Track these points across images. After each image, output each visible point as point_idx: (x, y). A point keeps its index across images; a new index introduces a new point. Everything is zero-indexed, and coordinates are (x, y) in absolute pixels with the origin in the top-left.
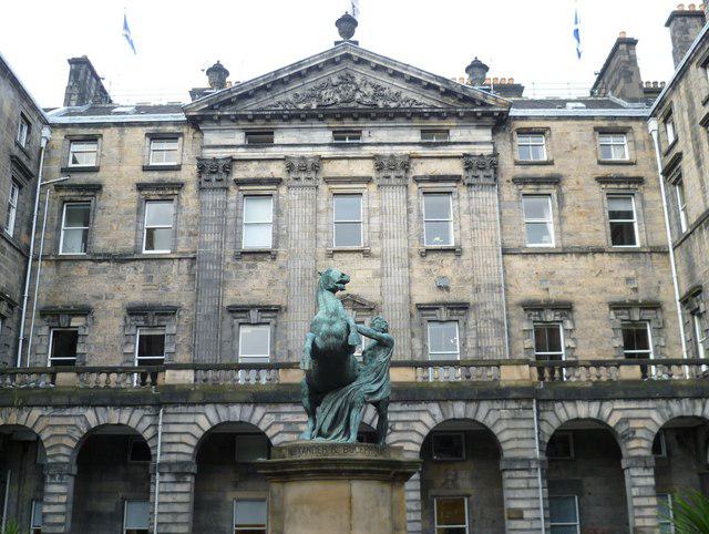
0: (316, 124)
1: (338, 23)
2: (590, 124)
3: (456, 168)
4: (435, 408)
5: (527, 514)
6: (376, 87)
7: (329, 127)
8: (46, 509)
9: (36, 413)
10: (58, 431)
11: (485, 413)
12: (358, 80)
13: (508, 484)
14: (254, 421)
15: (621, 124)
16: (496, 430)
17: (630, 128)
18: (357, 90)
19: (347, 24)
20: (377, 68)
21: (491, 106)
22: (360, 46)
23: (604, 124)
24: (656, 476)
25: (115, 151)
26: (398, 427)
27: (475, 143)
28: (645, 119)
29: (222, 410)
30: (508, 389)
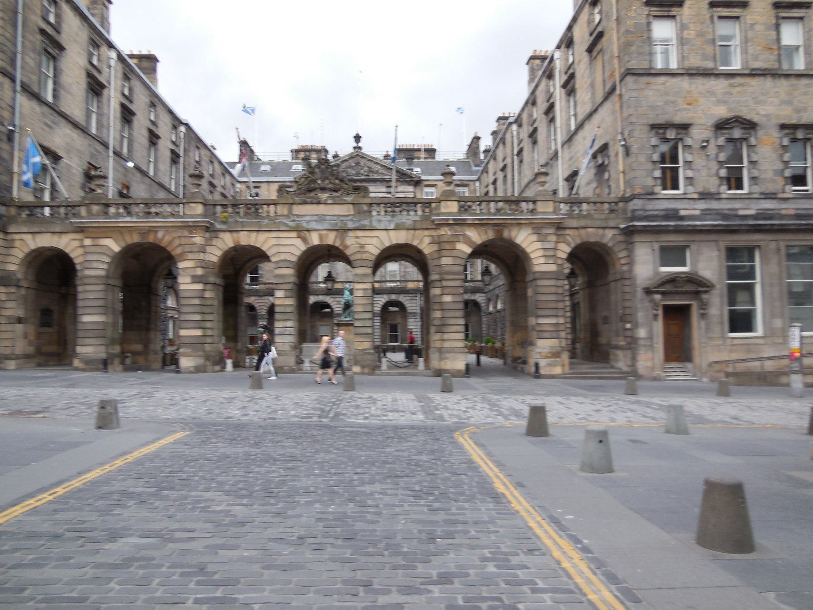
4: (385, 296)
6: (369, 168)
9: (253, 298)
10: (262, 304)
11: (402, 298)
12: (362, 164)
15: (465, 183)
19: (358, 138)
20: (370, 160)
23: (458, 183)
30: (409, 290)
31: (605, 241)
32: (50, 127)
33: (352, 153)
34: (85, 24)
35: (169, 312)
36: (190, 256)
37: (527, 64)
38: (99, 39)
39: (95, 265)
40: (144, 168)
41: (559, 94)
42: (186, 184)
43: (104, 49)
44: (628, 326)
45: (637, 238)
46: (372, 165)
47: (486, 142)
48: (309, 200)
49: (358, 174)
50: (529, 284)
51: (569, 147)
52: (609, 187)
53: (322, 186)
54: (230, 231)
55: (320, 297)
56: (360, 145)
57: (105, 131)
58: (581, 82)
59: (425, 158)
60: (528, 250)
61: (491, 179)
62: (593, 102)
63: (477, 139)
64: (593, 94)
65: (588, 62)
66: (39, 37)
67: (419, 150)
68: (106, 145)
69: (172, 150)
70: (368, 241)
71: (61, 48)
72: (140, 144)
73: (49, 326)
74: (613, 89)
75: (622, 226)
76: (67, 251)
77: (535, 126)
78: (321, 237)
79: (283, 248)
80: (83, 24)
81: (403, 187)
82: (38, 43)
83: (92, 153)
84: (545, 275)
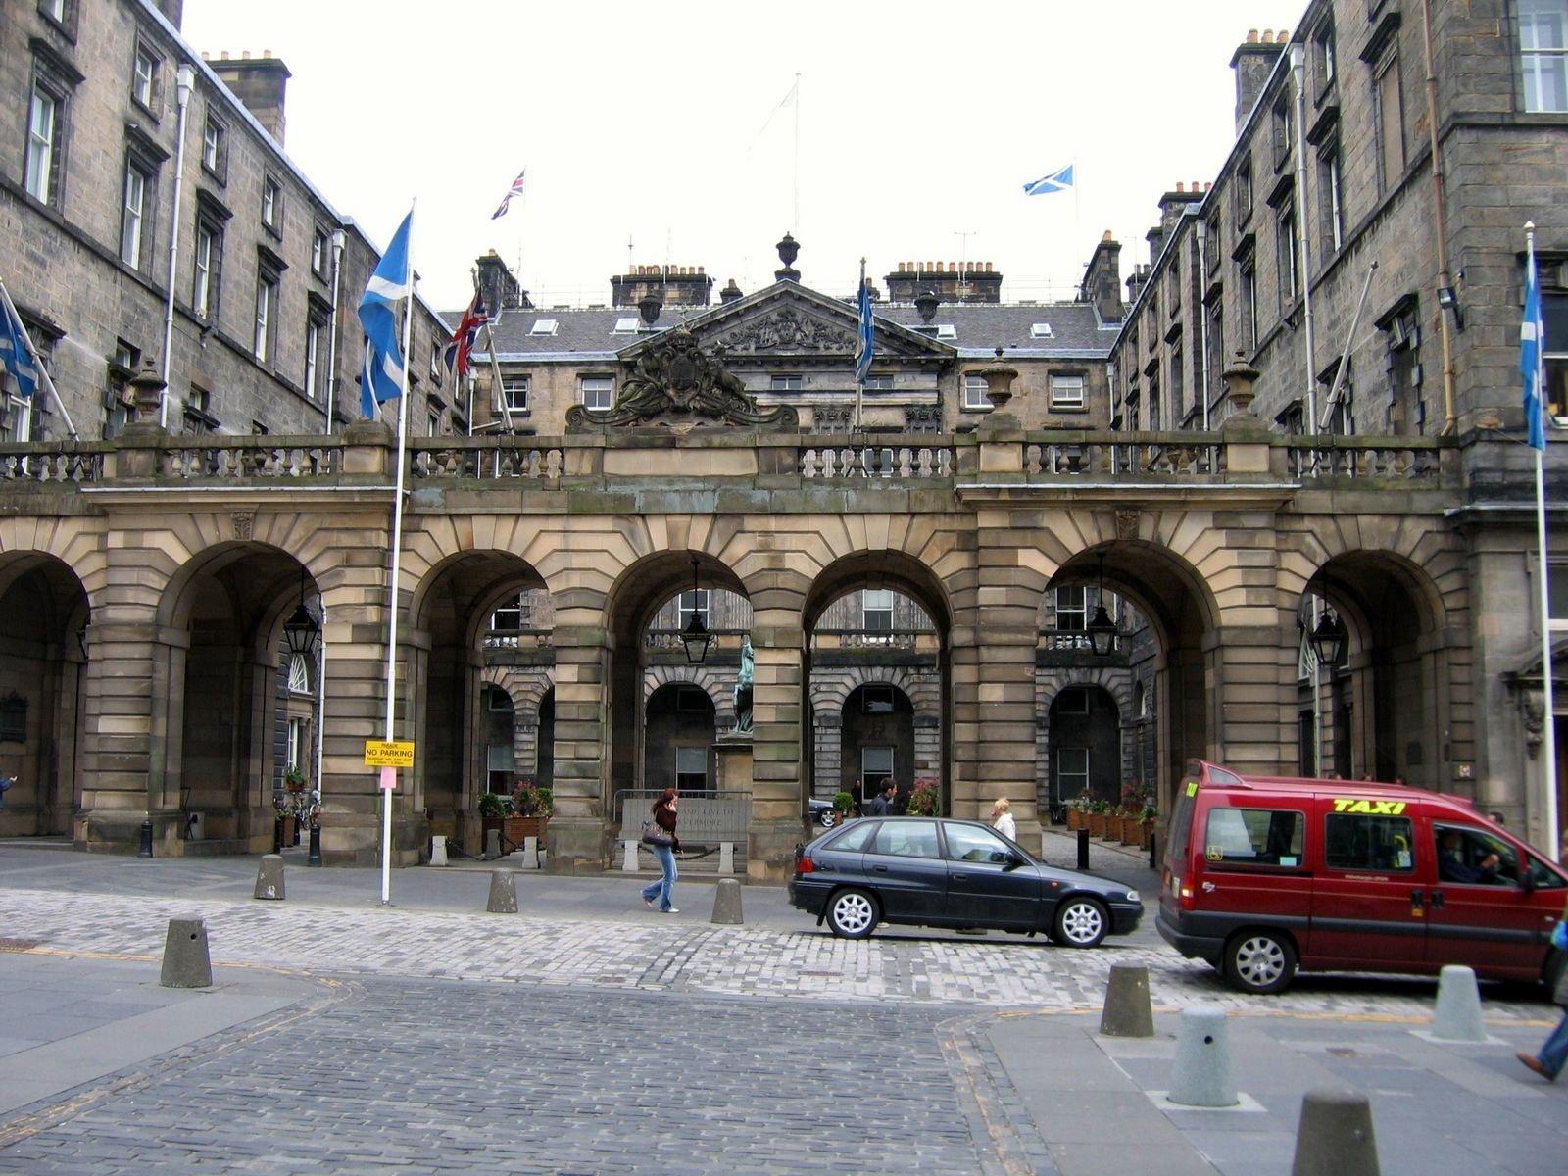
0: (754, 369)
1: (780, 246)
2: (1045, 367)
3: (895, 418)
4: (856, 672)
5: (931, 765)
6: (819, 326)
7: (768, 373)
8: (517, 755)
9: (503, 671)
10: (523, 687)
12: (799, 317)
13: (918, 739)
14: (697, 681)
15: (1078, 366)
16: (909, 692)
17: (1087, 371)
18: (798, 329)
19: (788, 249)
20: (818, 306)
21: (936, 353)
22: (803, 282)
23: (1060, 366)
24: (1050, 736)
25: (546, 392)
26: (823, 688)
27: (919, 391)
28: (1103, 361)
29: (669, 672)
31: (1404, 548)
32: (43, 264)
33: (773, 288)
34: (130, 16)
35: (290, 704)
36: (351, 576)
37: (1234, 63)
38: (156, 45)
39: (131, 596)
40: (245, 344)
41: (1303, 158)
42: (343, 376)
43: (168, 66)
44: (1465, 771)
45: (1487, 544)
46: (825, 319)
47: (1135, 256)
49: (786, 343)
50: (1209, 656)
51: (1330, 295)
52: (1422, 405)
53: (679, 402)
55: (681, 671)
56: (794, 266)
57: (159, 260)
58: (1354, 133)
59: (971, 299)
60: (1204, 570)
61: (1145, 360)
62: (1382, 185)
63: (1108, 250)
64: (1381, 165)
65: (1368, 85)
66: (28, 57)
67: (951, 277)
68: (160, 296)
69: (311, 294)
70: (792, 542)
71: (75, 78)
72: (237, 284)
73: (20, 739)
74: (1425, 160)
75: (1447, 512)
76: (69, 561)
77: (1250, 230)
78: (672, 534)
79: (579, 561)
80: (123, 15)
81: (909, 377)
82: (27, 72)
83: (126, 317)
84: (1249, 637)
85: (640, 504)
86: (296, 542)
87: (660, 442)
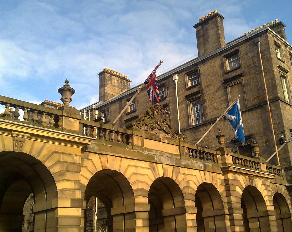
36: (69, 176)
48: (154, 137)
54: (99, 154)
79: (141, 176)
85: (156, 159)
86: (44, 156)
87: (157, 139)
